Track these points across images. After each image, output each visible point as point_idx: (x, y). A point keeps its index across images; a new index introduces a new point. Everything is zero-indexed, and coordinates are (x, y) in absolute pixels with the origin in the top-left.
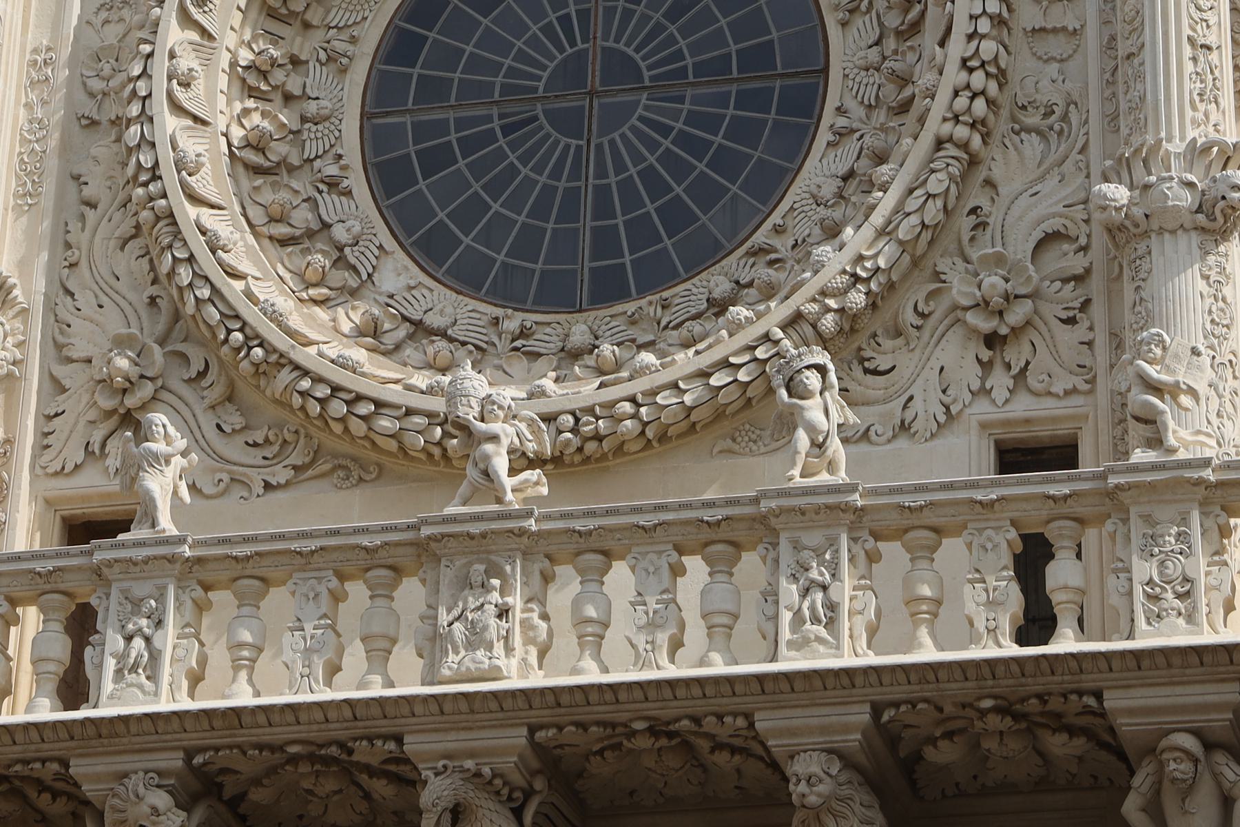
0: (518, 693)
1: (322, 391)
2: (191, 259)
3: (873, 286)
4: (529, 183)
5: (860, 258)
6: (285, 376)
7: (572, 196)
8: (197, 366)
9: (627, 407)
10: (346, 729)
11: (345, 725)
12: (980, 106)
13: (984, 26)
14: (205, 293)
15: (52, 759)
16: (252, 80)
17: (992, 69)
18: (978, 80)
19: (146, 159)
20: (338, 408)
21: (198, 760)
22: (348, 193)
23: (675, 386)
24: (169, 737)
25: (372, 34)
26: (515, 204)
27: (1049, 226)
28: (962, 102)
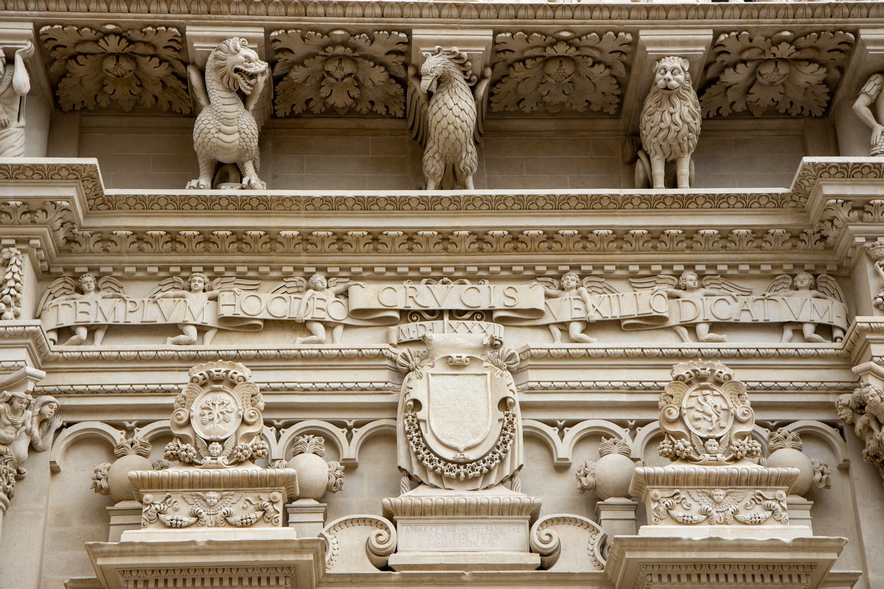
0: (492, 6)
10: (376, 22)
11: (376, 19)
15: (173, 26)
21: (274, 34)
24: (256, 17)
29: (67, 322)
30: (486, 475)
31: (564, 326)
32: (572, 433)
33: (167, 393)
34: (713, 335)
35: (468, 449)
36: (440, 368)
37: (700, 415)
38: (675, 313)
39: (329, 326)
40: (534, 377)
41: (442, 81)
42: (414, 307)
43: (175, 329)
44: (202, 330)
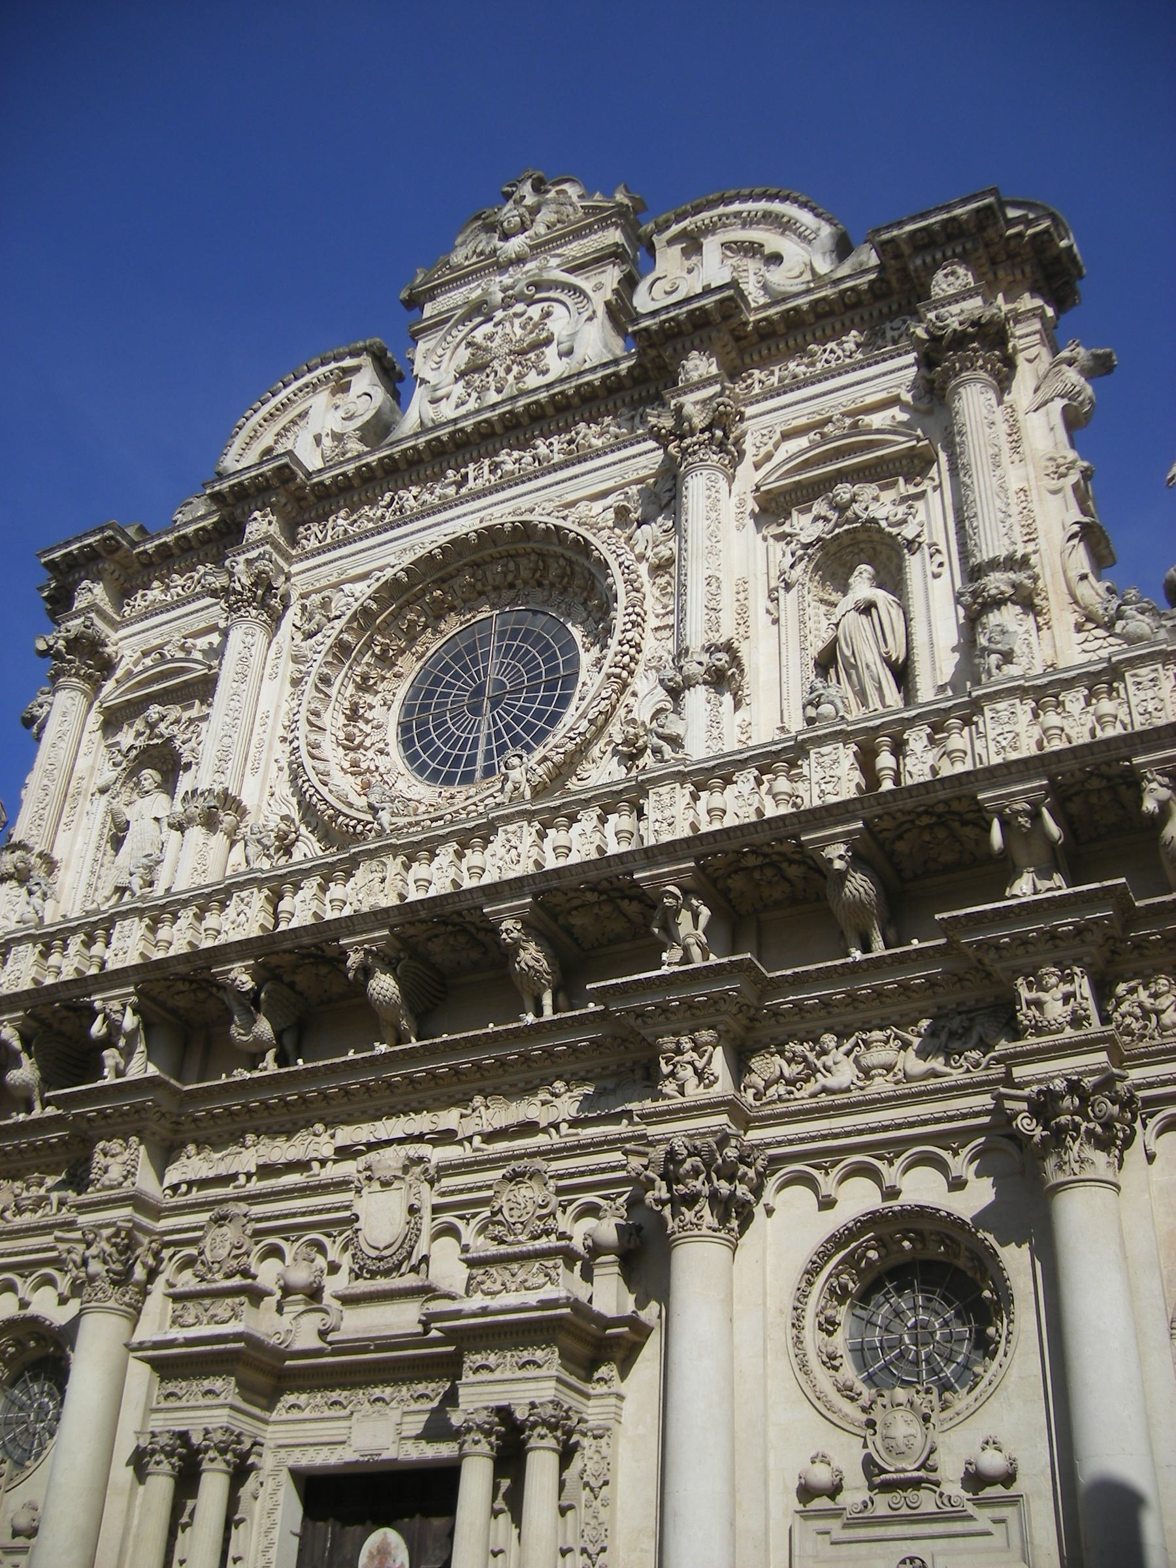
1: (353, 823)
2: (309, 780)
3: (578, 740)
4: (467, 739)
5: (572, 729)
6: (341, 818)
7: (476, 740)
8: (314, 825)
9: (473, 807)
12: (627, 659)
13: (629, 626)
14: (312, 791)
16: (348, 712)
17: (633, 643)
18: (626, 648)
19: (295, 744)
20: (360, 828)
22: (388, 754)
23: (492, 795)
25: (402, 692)
26: (452, 747)
27: (658, 706)
28: (619, 658)
29: (175, 1181)
30: (401, 1263)
31: (469, 1139)
32: (473, 1222)
33: (194, 1229)
34: (572, 1131)
35: (386, 1248)
36: (376, 1186)
37: (515, 1205)
38: (543, 1116)
39: (323, 1163)
40: (447, 1183)
41: (366, 972)
42: (373, 1140)
43: (234, 1177)
44: (249, 1176)
